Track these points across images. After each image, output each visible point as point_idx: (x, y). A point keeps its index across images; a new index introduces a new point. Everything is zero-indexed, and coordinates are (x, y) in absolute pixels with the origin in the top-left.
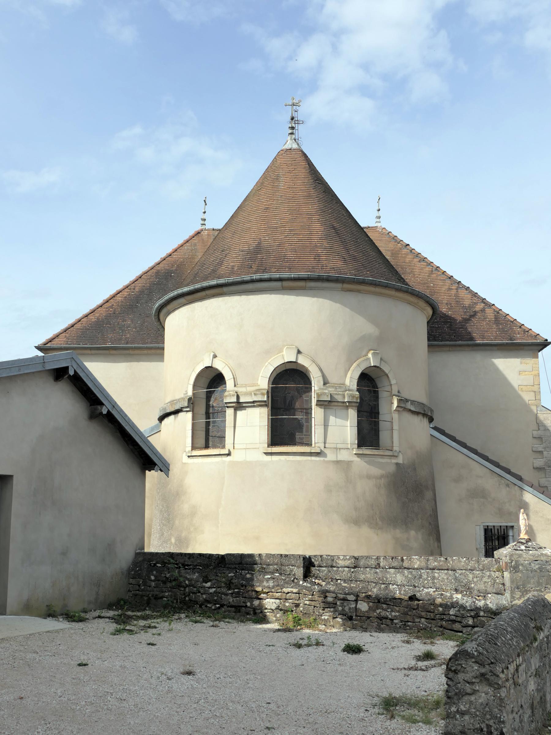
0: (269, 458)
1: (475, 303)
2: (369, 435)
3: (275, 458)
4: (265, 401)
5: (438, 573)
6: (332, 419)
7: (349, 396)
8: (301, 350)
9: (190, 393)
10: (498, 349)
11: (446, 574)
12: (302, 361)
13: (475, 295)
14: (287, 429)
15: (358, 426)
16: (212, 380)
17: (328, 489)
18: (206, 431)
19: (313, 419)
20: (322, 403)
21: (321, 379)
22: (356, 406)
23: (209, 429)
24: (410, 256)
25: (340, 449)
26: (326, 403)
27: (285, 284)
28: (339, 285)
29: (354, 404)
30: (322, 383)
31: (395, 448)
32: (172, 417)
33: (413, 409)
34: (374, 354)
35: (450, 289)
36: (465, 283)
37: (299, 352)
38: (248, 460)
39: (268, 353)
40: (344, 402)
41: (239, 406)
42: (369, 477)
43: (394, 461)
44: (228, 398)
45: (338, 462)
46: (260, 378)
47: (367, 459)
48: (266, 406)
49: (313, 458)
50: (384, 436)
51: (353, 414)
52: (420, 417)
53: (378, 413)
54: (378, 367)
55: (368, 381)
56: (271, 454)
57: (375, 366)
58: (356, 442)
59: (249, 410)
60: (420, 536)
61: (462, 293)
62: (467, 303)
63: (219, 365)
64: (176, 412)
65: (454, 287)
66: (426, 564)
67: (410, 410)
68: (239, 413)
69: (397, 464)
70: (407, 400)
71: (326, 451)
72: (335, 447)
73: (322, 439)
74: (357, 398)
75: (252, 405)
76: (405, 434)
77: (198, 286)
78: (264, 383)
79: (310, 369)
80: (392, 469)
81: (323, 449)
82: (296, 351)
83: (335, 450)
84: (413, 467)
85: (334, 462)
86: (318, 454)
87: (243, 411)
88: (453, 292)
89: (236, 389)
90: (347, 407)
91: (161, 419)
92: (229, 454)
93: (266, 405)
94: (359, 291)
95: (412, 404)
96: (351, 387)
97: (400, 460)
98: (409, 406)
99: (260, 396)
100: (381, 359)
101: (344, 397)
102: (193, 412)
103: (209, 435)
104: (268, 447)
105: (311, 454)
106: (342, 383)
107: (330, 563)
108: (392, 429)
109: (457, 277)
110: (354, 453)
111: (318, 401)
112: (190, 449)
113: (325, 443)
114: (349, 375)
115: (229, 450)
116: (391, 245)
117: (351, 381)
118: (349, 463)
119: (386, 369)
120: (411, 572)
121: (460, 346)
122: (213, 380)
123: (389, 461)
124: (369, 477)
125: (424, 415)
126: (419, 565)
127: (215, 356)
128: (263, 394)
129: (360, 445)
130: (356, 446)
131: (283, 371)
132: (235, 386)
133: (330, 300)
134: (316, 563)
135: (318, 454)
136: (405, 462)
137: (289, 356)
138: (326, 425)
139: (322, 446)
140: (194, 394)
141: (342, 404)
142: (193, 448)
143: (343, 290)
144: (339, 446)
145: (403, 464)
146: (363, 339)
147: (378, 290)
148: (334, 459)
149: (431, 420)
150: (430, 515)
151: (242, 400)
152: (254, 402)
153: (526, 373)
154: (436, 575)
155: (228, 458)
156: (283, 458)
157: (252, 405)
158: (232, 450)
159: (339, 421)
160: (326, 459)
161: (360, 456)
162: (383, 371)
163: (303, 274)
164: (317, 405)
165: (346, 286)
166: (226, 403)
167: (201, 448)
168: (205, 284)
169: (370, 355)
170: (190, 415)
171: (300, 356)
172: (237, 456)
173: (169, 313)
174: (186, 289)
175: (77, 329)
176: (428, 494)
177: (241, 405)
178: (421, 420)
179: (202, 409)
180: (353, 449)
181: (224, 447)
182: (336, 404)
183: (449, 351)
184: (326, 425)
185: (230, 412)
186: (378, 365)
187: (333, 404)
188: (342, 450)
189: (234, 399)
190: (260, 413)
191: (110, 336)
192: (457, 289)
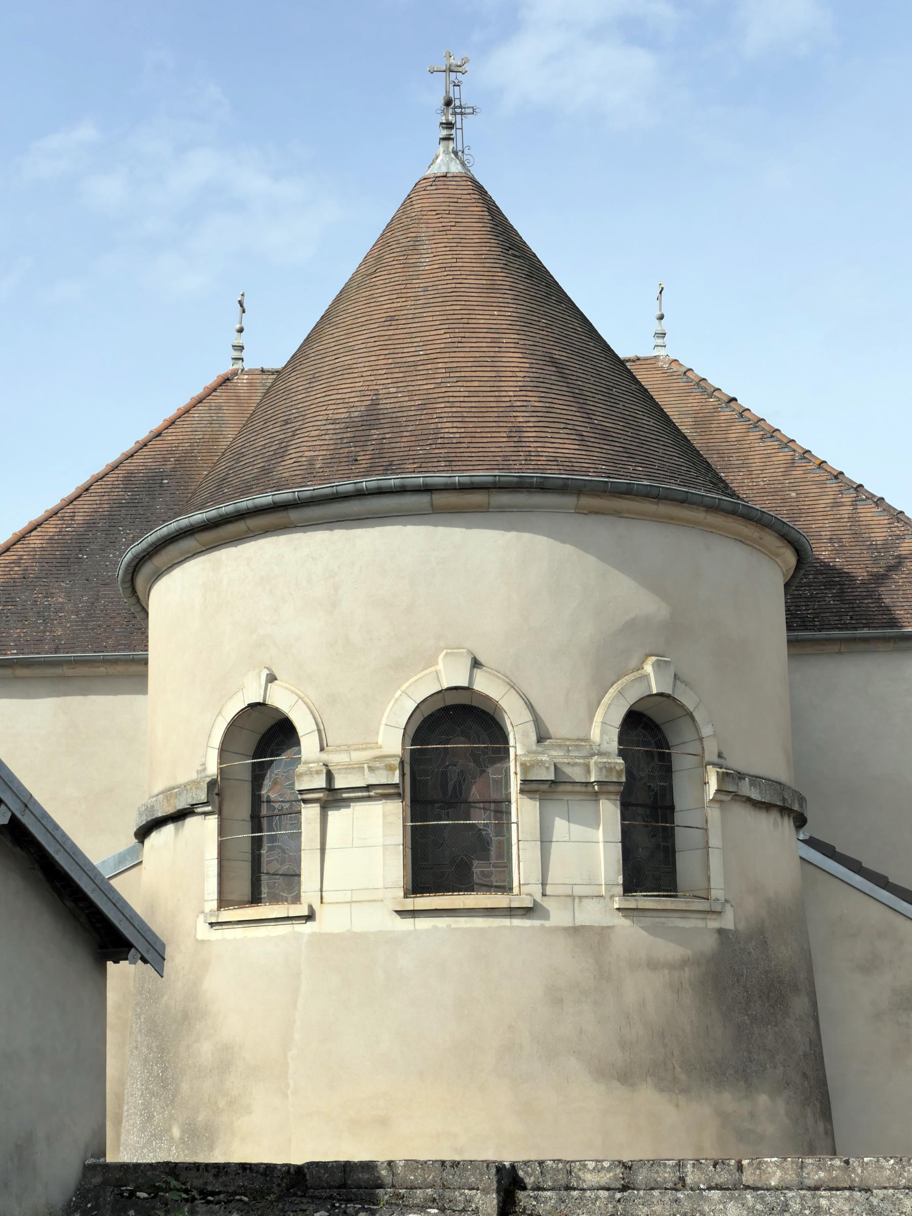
0: (407, 924)
1: (899, 537)
2: (650, 864)
4: (396, 786)
5: (829, 1198)
6: (560, 826)
7: (601, 769)
8: (481, 659)
9: (213, 769)
11: (847, 1199)
12: (484, 685)
13: (898, 516)
14: (449, 853)
15: (623, 842)
16: (266, 736)
17: (555, 997)
19: (514, 827)
20: (534, 786)
22: (616, 793)
23: (260, 855)
24: (739, 428)
25: (581, 897)
26: (545, 787)
27: (440, 499)
28: (570, 501)
29: (612, 788)
30: (533, 737)
31: (714, 894)
32: (169, 829)
33: (755, 795)
34: (657, 665)
35: (837, 504)
36: (874, 488)
37: (476, 664)
38: (357, 929)
39: (401, 668)
40: (587, 784)
41: (332, 798)
42: (653, 965)
43: (713, 924)
44: (306, 778)
45: (576, 931)
47: (647, 921)
48: (400, 796)
49: (517, 922)
50: (686, 864)
51: (609, 811)
52: (774, 815)
53: (672, 808)
54: (668, 696)
55: (648, 731)
56: (414, 913)
57: (661, 695)
58: (620, 880)
59: (359, 809)
60: (781, 1107)
61: (868, 513)
62: (879, 535)
63: (281, 699)
64: (179, 816)
65: (847, 498)
66: (799, 1175)
67: (749, 800)
68: (333, 815)
69: (721, 931)
70: (741, 776)
71: (546, 903)
72: (570, 893)
73: (536, 876)
74: (619, 773)
76: (738, 858)
77: (227, 508)
78: (392, 741)
79: (503, 704)
80: (709, 943)
81: (538, 898)
82: (468, 663)
83: (569, 900)
84: (760, 936)
85: (566, 929)
86: (527, 912)
87: (343, 811)
88: (846, 511)
89: (324, 757)
90: (596, 796)
91: (143, 833)
92: (310, 917)
94: (618, 513)
95: (752, 784)
96: (605, 747)
97: (728, 922)
98: (746, 789)
100: (675, 675)
101: (588, 771)
102: (220, 814)
103: (259, 873)
104: (406, 896)
105: (510, 912)
106: (581, 736)
107: (562, 1179)
109: (854, 475)
110: (616, 906)
111: (524, 782)
112: (214, 905)
113: (544, 884)
114: (598, 717)
115: (311, 908)
116: (694, 401)
117: (603, 732)
118: (603, 933)
119: (688, 700)
120: (762, 1198)
121: (865, 640)
122: (266, 736)
123: (700, 924)
124: (653, 965)
125: (784, 810)
126: (782, 1179)
127: (272, 678)
128: (390, 768)
129: (629, 888)
130: (620, 890)
131: (439, 711)
132: (322, 749)
133: (549, 535)
134: (529, 1181)
135: (527, 912)
136: (742, 926)
137: (451, 674)
138: (545, 841)
139: (537, 890)
140: (221, 771)
141: (583, 789)
142: (223, 902)
143: (580, 511)
144: (578, 891)
145: (736, 931)
146: (632, 628)
147: (664, 509)
149: (800, 821)
150: (805, 1055)
151: (339, 784)
152: (368, 788)
154: (824, 1202)
155: (309, 927)
156: (442, 922)
158: (316, 906)
159: (577, 830)
160: (547, 924)
161: (631, 913)
162: (682, 706)
163: (482, 475)
164: (522, 791)
165: (585, 501)
166: (301, 792)
167: (241, 904)
168: (245, 503)
169: (648, 668)
170: (212, 822)
171: (478, 673)
172: (330, 921)
173: (158, 575)
174: (198, 517)
176: (799, 1004)
177: (338, 797)
178: (775, 824)
179: (241, 809)
180: (612, 897)
181: (297, 899)
182: (569, 788)
183: (840, 653)
184: (545, 841)
185: (310, 814)
186: (669, 691)
187: (562, 788)
188: (585, 901)
189: (320, 782)
190: (384, 816)
191: (15, 633)
192: (854, 503)
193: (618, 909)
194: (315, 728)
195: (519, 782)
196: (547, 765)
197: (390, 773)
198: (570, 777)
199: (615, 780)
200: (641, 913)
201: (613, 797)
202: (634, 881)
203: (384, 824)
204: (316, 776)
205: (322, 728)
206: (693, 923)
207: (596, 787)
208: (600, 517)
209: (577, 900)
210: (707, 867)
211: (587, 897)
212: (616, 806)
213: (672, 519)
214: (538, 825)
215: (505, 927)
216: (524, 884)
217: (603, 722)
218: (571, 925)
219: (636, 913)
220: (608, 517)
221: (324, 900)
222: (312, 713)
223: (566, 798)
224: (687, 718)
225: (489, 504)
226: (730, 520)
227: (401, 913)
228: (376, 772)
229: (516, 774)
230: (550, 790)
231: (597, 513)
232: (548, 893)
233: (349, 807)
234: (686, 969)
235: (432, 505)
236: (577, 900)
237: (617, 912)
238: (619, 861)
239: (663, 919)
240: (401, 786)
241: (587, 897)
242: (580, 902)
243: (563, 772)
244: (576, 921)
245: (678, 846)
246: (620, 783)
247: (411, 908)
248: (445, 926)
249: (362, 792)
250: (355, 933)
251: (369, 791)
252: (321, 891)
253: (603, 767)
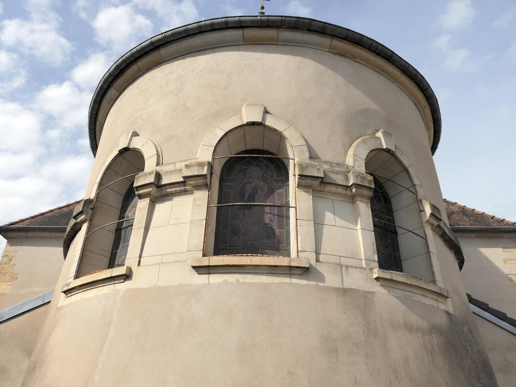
0: (203, 279)
3: (216, 279)
4: (204, 176)
6: (329, 217)
7: (357, 176)
10: (477, 237)
18: (111, 258)
19: (292, 211)
20: (308, 181)
21: (305, 149)
23: (116, 253)
26: (317, 183)
28: (326, 41)
30: (307, 155)
34: (385, 133)
37: (266, 112)
38: (162, 284)
39: (217, 116)
40: (347, 187)
42: (409, 328)
44: (141, 179)
45: (345, 291)
46: (201, 145)
47: (399, 293)
48: (207, 186)
57: (388, 151)
58: (376, 258)
59: (177, 200)
68: (161, 208)
71: (320, 268)
72: (338, 262)
73: (311, 245)
75: (183, 188)
79: (286, 133)
80: (442, 320)
81: (313, 263)
83: (338, 268)
85: (337, 289)
87: (167, 203)
89: (159, 169)
90: (353, 199)
92: (127, 276)
93: (206, 185)
99: (197, 168)
101: (347, 179)
102: (91, 221)
104: (204, 255)
105: (291, 271)
106: (340, 162)
108: (428, 252)
110: (375, 276)
111: (302, 176)
113: (317, 253)
114: (351, 152)
117: (354, 160)
124: (409, 328)
127: (135, 134)
132: (158, 164)
133: (314, 60)
135: (305, 271)
138: (318, 224)
140: (98, 195)
141: (344, 192)
144: (345, 261)
146: (365, 112)
148: (338, 284)
153: (512, 261)
155: (127, 285)
157: (183, 188)
158: (134, 269)
159: (340, 222)
160: (321, 284)
161: (387, 283)
164: (299, 186)
165: (336, 43)
169: (380, 134)
171: (268, 117)
175: (47, 217)
177: (164, 192)
180: (371, 269)
182: (333, 189)
184: (318, 224)
187: (328, 188)
188: (350, 269)
190: (194, 200)
193: (377, 279)
194: (155, 153)
195: (297, 177)
196: (318, 167)
197: (201, 168)
198: (335, 181)
199: (367, 185)
201: (366, 201)
202: (383, 264)
203: (193, 206)
204: (148, 176)
205: (160, 154)
206: (429, 301)
207: (354, 190)
208: (343, 58)
209: (344, 268)
210: (431, 266)
211: (352, 267)
212: (367, 206)
213: (383, 71)
214: (312, 210)
215: (285, 283)
216: (301, 251)
217: (354, 155)
218: (340, 286)
219: (390, 284)
220: (347, 60)
221: (141, 264)
222: (155, 146)
223: (331, 197)
224: (404, 174)
225: (278, 37)
226: (412, 85)
227: (199, 269)
228: (191, 168)
229: (295, 175)
230: (319, 189)
231: (342, 55)
232: (321, 260)
233: (171, 200)
234: (433, 335)
235: (243, 37)
236: (344, 268)
237: (375, 282)
238: (373, 244)
239: (410, 294)
240: (208, 177)
241: (352, 267)
242: (347, 270)
243: (329, 177)
244: (345, 284)
245: (402, 258)
247: (207, 264)
248: (234, 280)
249: (180, 187)
250: (159, 287)
251: (185, 186)
252: (140, 257)
253: (358, 175)
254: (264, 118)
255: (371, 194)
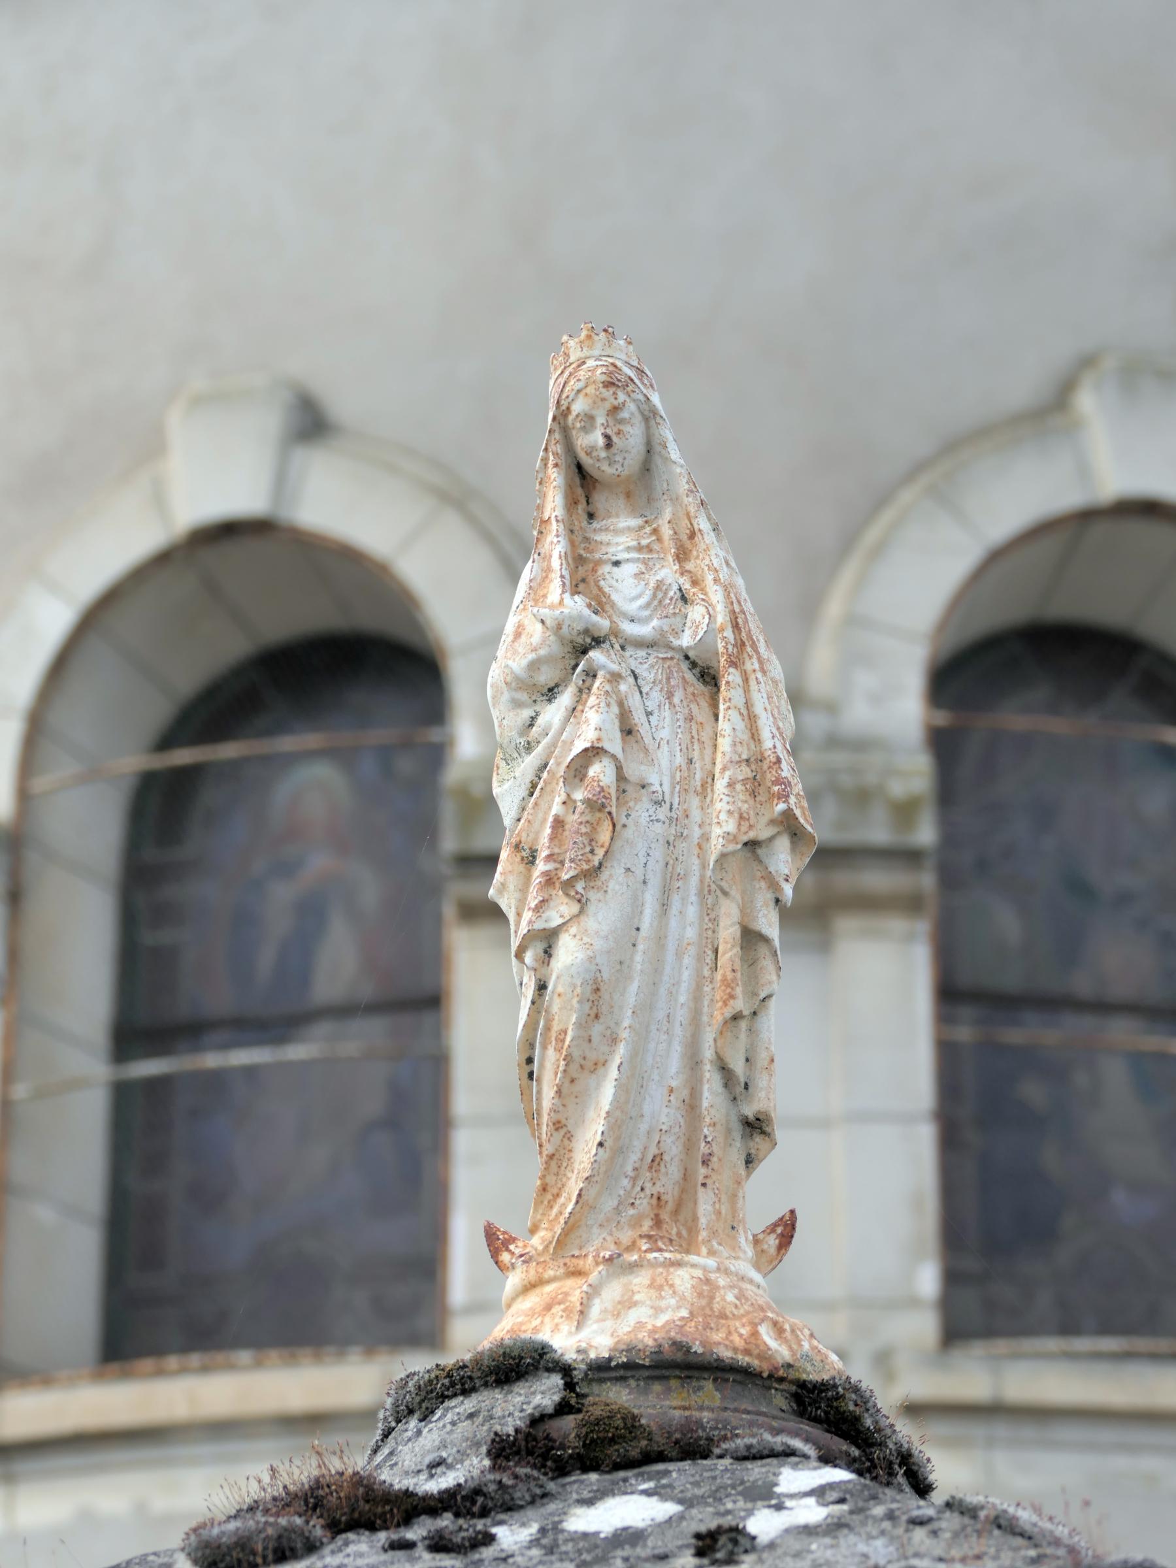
8: (342, 404)
12: (337, 503)
22: (911, 904)
29: (877, 880)
37: (310, 423)
58: (928, 1280)
74: (904, 812)
96: (859, 715)
130: (924, 1326)
137: (216, 477)
200: (1029, 1431)
201: (897, 924)
246: (911, 857)
254: (281, 482)
255: (927, 881)
